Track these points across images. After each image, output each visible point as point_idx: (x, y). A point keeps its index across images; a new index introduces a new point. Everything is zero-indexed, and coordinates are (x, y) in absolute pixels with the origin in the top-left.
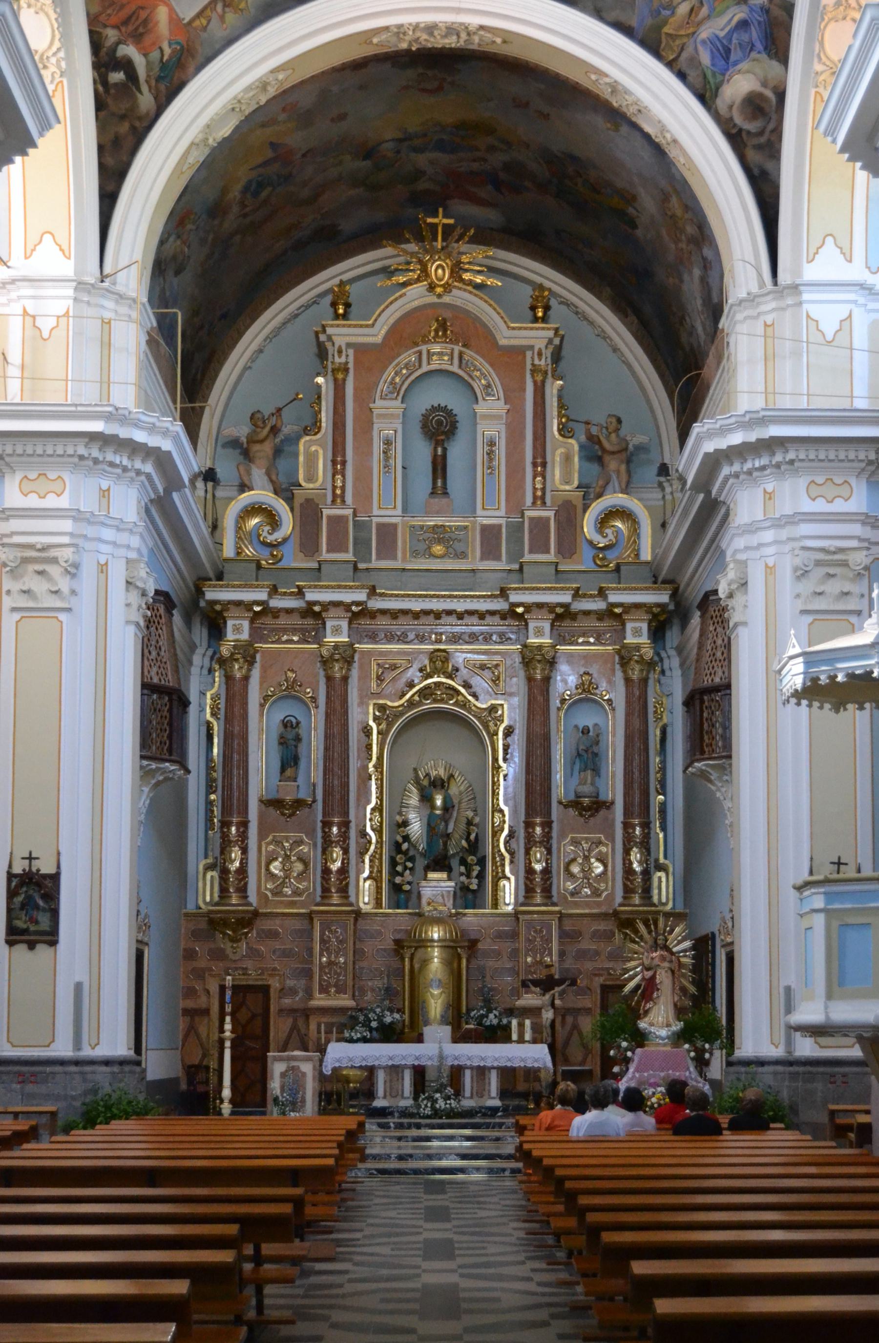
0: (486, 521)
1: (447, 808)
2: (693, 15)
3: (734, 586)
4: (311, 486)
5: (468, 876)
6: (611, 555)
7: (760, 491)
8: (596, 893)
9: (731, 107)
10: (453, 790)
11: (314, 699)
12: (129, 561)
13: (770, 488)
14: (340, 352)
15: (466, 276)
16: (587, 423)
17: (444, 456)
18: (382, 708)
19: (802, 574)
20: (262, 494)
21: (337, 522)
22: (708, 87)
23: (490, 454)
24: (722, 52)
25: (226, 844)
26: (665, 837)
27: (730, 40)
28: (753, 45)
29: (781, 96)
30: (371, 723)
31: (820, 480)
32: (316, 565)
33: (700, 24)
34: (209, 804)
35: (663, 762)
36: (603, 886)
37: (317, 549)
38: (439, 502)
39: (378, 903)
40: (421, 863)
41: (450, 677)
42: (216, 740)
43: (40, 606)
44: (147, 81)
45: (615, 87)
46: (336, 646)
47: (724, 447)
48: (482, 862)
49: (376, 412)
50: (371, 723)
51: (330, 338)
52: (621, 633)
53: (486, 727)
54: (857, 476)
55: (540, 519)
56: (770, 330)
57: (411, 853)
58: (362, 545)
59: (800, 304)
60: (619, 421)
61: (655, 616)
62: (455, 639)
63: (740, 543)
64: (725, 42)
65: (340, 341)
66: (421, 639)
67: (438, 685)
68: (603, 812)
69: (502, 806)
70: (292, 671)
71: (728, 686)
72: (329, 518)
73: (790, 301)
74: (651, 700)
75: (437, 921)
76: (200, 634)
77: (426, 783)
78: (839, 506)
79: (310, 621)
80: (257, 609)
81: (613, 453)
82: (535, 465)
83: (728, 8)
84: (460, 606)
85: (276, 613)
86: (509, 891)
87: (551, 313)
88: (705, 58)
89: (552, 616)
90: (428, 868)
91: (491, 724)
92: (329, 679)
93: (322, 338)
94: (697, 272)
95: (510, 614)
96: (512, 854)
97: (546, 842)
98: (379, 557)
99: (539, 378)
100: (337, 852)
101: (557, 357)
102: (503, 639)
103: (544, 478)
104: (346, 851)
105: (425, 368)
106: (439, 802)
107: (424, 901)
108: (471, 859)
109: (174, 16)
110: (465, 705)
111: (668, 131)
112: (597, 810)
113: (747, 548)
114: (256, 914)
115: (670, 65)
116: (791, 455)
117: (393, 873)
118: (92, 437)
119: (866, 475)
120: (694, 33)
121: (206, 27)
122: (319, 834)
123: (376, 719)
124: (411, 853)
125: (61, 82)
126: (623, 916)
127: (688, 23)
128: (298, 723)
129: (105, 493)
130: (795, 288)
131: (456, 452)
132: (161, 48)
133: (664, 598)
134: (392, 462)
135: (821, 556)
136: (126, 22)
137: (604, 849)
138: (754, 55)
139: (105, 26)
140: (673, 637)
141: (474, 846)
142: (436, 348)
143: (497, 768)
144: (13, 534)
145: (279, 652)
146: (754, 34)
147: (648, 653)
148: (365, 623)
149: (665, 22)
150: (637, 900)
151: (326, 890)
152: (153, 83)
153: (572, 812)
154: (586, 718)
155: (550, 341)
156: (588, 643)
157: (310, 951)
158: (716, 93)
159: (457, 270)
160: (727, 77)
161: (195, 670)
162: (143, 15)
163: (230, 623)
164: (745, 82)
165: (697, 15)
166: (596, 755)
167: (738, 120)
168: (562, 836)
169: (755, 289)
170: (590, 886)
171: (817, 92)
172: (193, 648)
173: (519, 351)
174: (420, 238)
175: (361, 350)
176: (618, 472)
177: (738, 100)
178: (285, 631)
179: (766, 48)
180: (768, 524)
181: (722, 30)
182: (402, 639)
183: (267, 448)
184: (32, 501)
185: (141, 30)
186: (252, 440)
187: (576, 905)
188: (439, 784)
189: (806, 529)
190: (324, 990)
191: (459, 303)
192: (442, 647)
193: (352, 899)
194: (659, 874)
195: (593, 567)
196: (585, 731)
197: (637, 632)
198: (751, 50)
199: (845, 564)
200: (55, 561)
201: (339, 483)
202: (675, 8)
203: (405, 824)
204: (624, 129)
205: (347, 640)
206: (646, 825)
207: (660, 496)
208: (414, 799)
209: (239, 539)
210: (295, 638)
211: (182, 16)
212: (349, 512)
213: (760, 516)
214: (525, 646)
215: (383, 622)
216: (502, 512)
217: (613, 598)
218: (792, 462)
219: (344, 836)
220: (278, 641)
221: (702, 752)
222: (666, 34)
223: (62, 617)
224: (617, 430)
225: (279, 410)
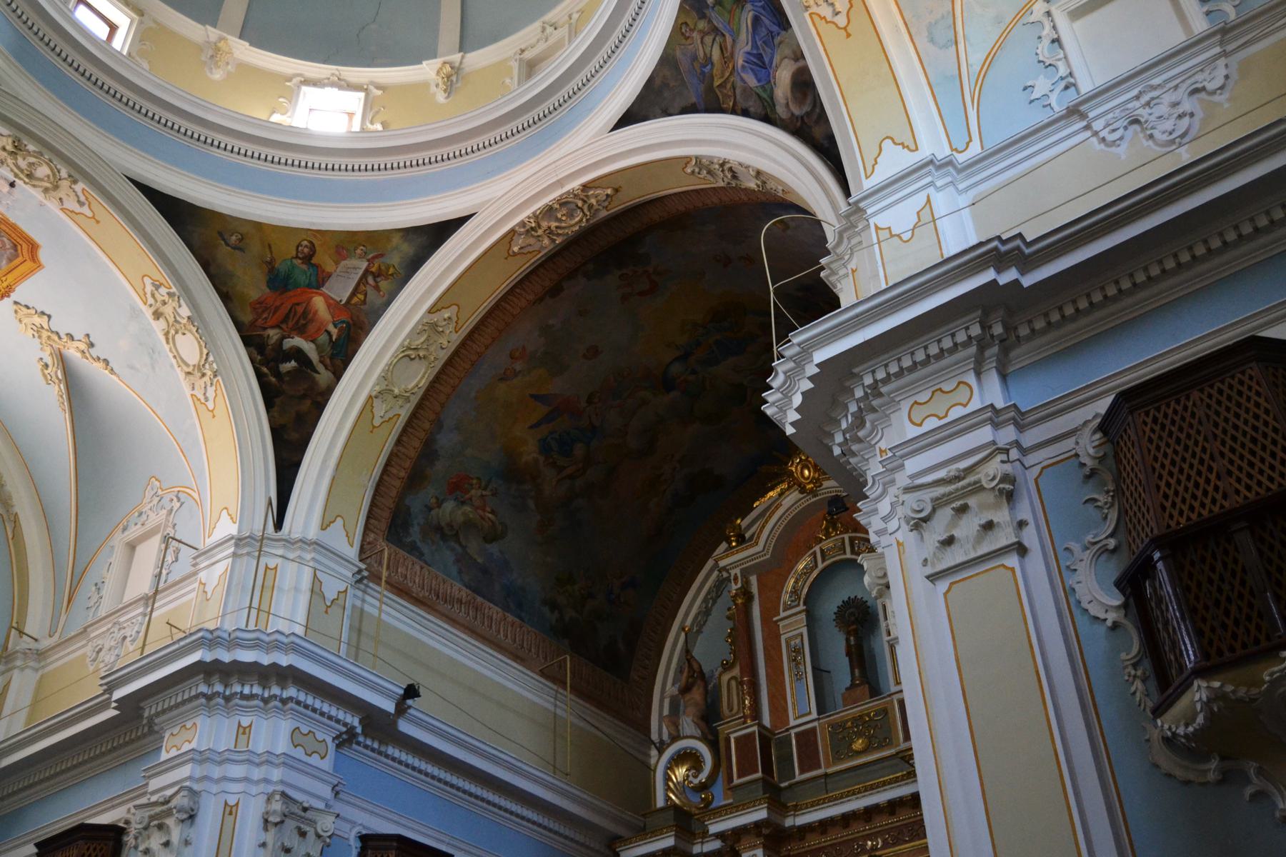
9: (787, 105)
22: (766, 104)
24: (757, 62)
27: (757, 48)
28: (772, 32)
44: (321, 362)
64: (755, 52)
88: (752, 81)
109: (331, 301)
115: (734, 112)
121: (365, 299)
125: (218, 381)
127: (725, 62)
132: (326, 331)
134: (802, 667)
136: (286, 319)
138: (777, 40)
139: (265, 329)
149: (712, 78)
152: (328, 361)
158: (772, 103)
162: (300, 310)
165: (726, 49)
177: (789, 95)
185: (302, 322)
198: (773, 38)
199: (977, 488)
202: (711, 57)
211: (338, 299)
222: (718, 86)
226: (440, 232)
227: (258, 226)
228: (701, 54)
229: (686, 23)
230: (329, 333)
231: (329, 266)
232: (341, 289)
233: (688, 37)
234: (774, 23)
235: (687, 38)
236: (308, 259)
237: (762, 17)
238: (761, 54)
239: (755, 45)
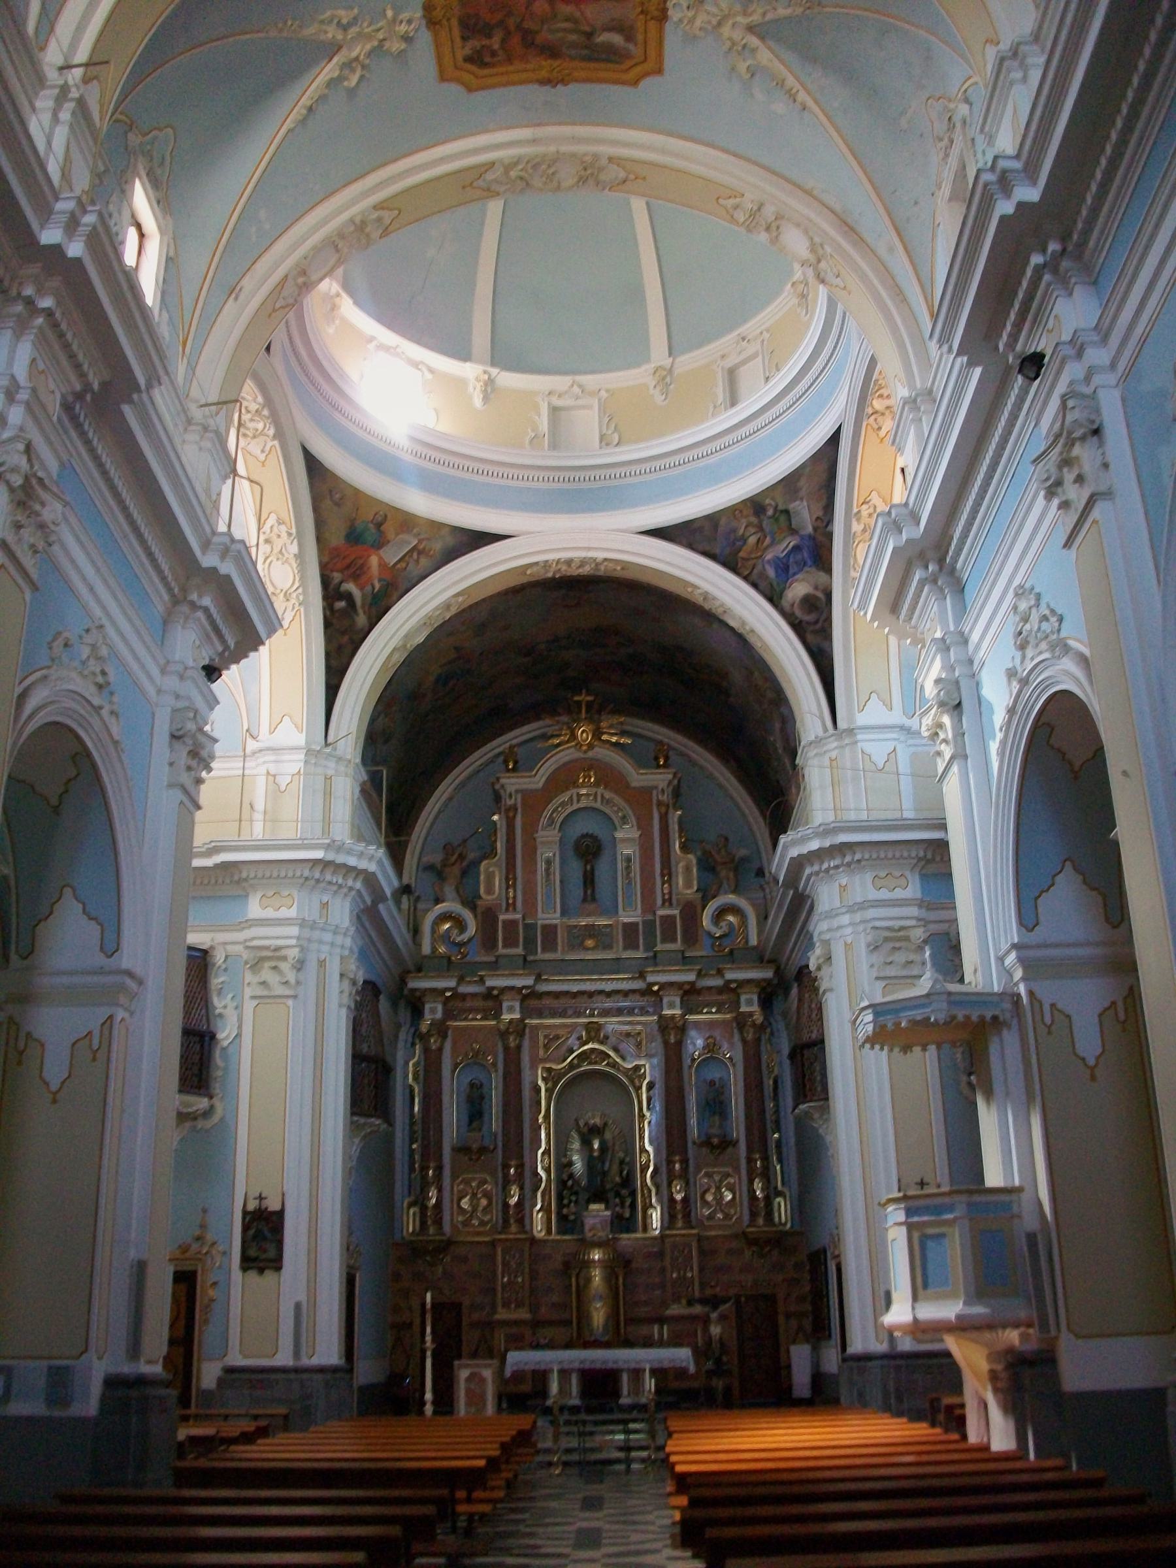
0: (626, 920)
1: (603, 1148)
3: (821, 960)
4: (489, 897)
5: (622, 1204)
6: (726, 942)
7: (837, 884)
8: (727, 1216)
9: (793, 605)
10: (608, 1136)
11: (494, 1064)
12: (342, 958)
13: (844, 882)
14: (510, 796)
15: (604, 737)
16: (702, 842)
17: (593, 869)
18: (549, 1070)
19: (874, 948)
20: (450, 905)
21: (511, 925)
23: (628, 868)
25: (425, 1186)
26: (782, 1167)
29: (829, 595)
30: (540, 1082)
31: (883, 874)
32: (493, 959)
34: (412, 1151)
35: (777, 1106)
36: (732, 1211)
37: (494, 946)
38: (591, 907)
39: (549, 1232)
40: (584, 1196)
41: (602, 1043)
42: (417, 1100)
43: (272, 993)
45: (706, 596)
46: (511, 1021)
47: (805, 852)
48: (633, 1194)
49: (538, 840)
50: (540, 1082)
51: (503, 786)
52: (737, 1004)
53: (632, 1082)
54: (912, 870)
55: (668, 916)
56: (834, 763)
57: (575, 1188)
58: (530, 943)
59: (856, 742)
60: (726, 839)
61: (764, 989)
62: (606, 1013)
63: (823, 926)
65: (511, 789)
66: (579, 1014)
67: (593, 1050)
68: (730, 1150)
69: (648, 1147)
70: (477, 1042)
71: (822, 1041)
72: (504, 922)
73: (847, 741)
74: (764, 1057)
75: (599, 1245)
76: (404, 1015)
77: (585, 1130)
78: (899, 894)
79: (490, 1004)
80: (448, 994)
81: (724, 863)
82: (663, 876)
84: (608, 987)
85: (464, 997)
86: (656, 1217)
87: (670, 762)
89: (681, 992)
90: (589, 1201)
91: (636, 1081)
92: (506, 1048)
93: (497, 787)
94: (777, 725)
95: (647, 992)
96: (657, 1187)
97: (684, 1175)
98: (544, 950)
99: (663, 810)
100: (514, 1190)
101: (677, 793)
102: (644, 1011)
103: (670, 886)
104: (521, 1188)
105: (575, 807)
106: (596, 1146)
107: (587, 1228)
108: (624, 1192)
110: (614, 1065)
112: (725, 1149)
113: (829, 930)
114: (450, 1243)
115: (746, 578)
116: (858, 856)
117: (560, 1205)
118: (316, 862)
119: (917, 870)
122: (500, 1175)
123: (544, 1079)
124: (575, 1188)
126: (751, 1236)
128: (481, 1085)
129: (325, 906)
130: (851, 732)
131: (602, 868)
133: (768, 974)
135: (887, 934)
137: (731, 1180)
138: (806, 569)
140: (778, 1006)
141: (627, 1181)
142: (584, 791)
143: (642, 1116)
144: (253, 939)
145: (466, 1028)
146: (806, 555)
147: (759, 1018)
148: (534, 1003)
149: (739, 551)
150: (761, 1221)
151: (506, 1221)
153: (704, 1150)
154: (714, 1074)
155: (670, 782)
156: (711, 1013)
157: (494, 1272)
159: (597, 734)
161: (401, 1044)
163: (427, 1006)
166: (721, 1103)
167: (798, 613)
168: (698, 1169)
169: (821, 733)
170: (722, 1211)
172: (398, 1026)
173: (647, 791)
174: (569, 711)
175: (526, 794)
176: (728, 879)
177: (798, 601)
178: (471, 1010)
180: (844, 910)
182: (563, 1014)
183: (456, 870)
184: (270, 913)
186: (445, 863)
187: (711, 1228)
188: (596, 1131)
189: (871, 913)
190: (506, 1305)
191: (599, 756)
192: (595, 1020)
193: (528, 1228)
194: (778, 1200)
195: (711, 953)
196: (712, 1083)
197: (749, 1002)
200: (285, 958)
201: (511, 894)
203: (570, 1164)
204: (715, 626)
205: (518, 1016)
206: (766, 1159)
207: (762, 895)
208: (576, 1145)
209: (434, 941)
210: (479, 1017)
212: (518, 916)
213: (838, 905)
214: (661, 1017)
215: (547, 1002)
216: (639, 911)
217: (730, 976)
218: (859, 861)
219: (520, 1175)
220: (466, 1019)
221: (805, 1096)
223: (290, 1002)
224: (725, 846)
225: (465, 841)
226: (480, 539)
227: (357, 492)
230: (373, 588)
231: (390, 534)
232: (392, 555)
236: (379, 525)
239: (788, 555)
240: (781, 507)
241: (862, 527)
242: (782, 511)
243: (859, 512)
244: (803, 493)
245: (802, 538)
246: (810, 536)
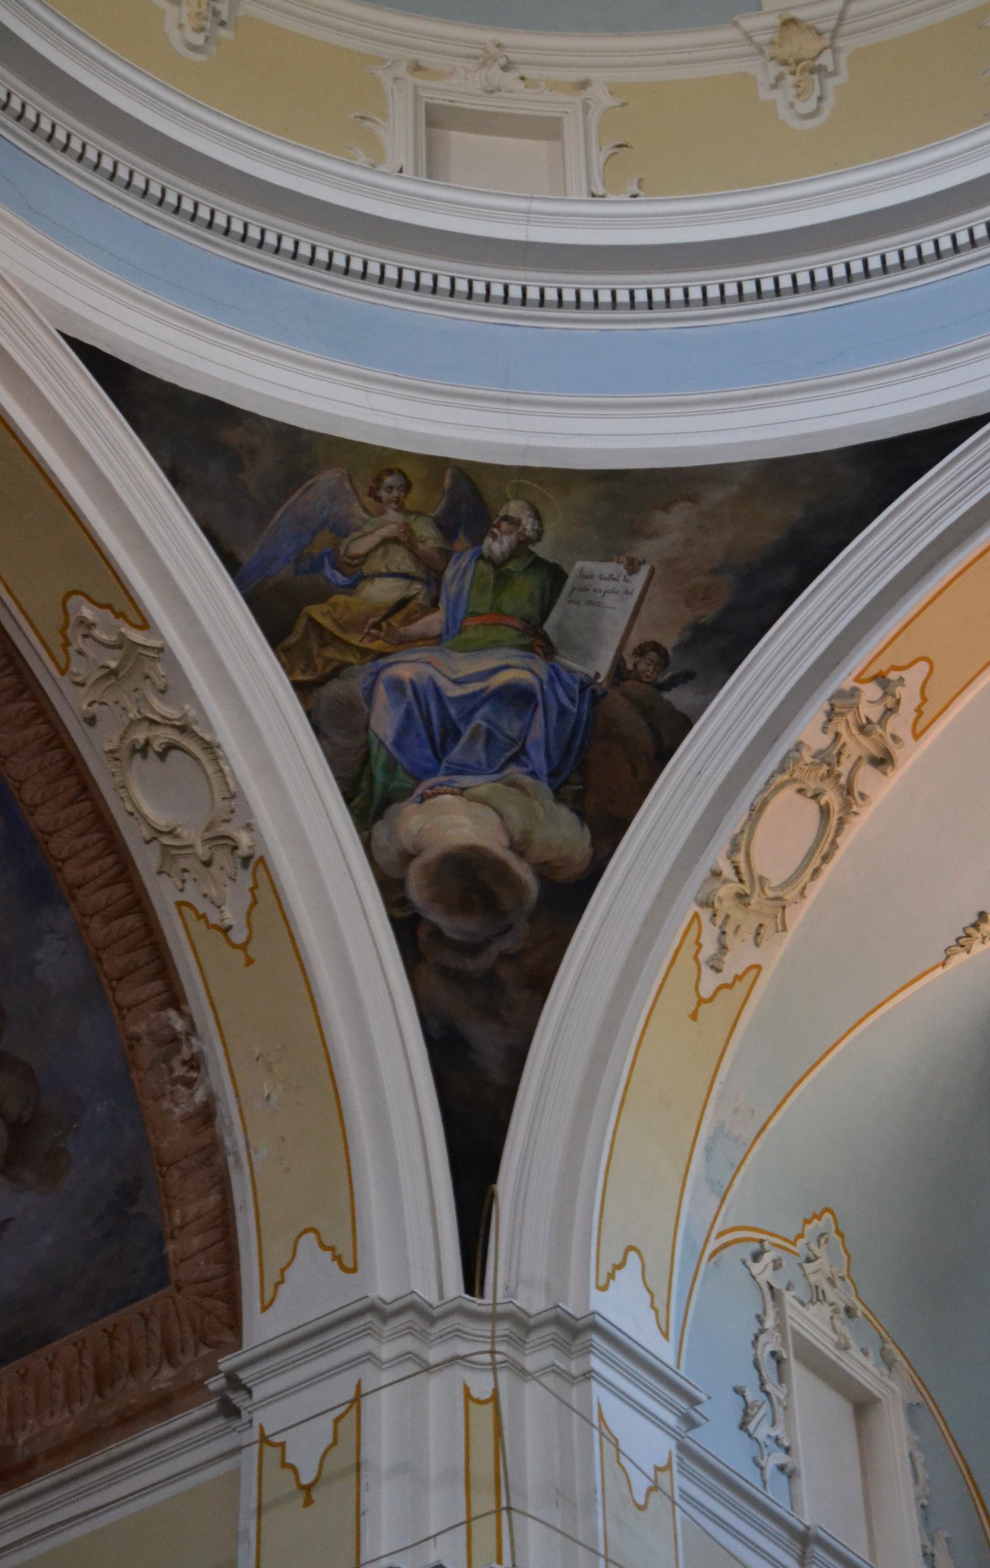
2: (399, 616)
9: (408, 857)
22: (364, 784)
27: (468, 716)
28: (523, 751)
33: (408, 642)
64: (453, 711)
83: (497, 644)
111: (249, 827)
120: (382, 655)
127: (377, 626)
138: (513, 771)
146: (537, 731)
149: (322, 596)
160: (422, 788)
164: (465, 820)
165: (408, 621)
167: (416, 891)
171: (696, 916)
177: (431, 854)
179: (553, 774)
181: (457, 682)
198: (514, 759)
202: (363, 578)
222: (312, 620)
228: (360, 547)
229: (407, 487)
233: (379, 499)
234: (548, 755)
235: (373, 493)
237: (540, 710)
238: (457, 734)
239: (470, 704)
240: (542, 550)
241: (823, 741)
242: (538, 562)
243: (854, 692)
244: (645, 549)
245: (556, 675)
246: (586, 684)
